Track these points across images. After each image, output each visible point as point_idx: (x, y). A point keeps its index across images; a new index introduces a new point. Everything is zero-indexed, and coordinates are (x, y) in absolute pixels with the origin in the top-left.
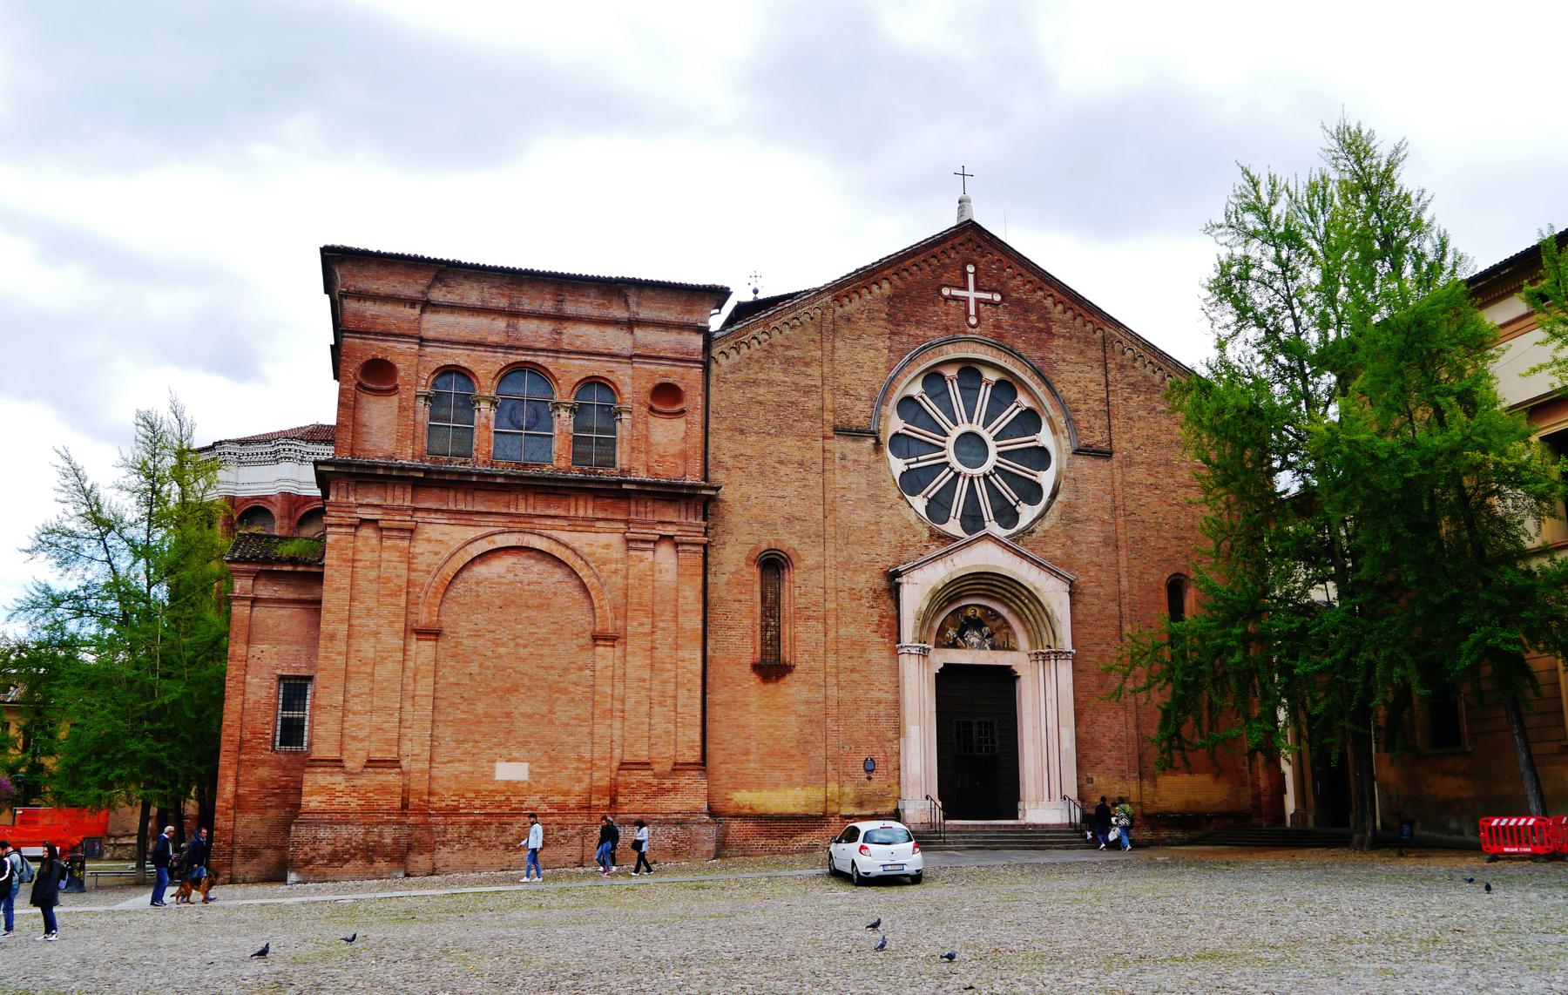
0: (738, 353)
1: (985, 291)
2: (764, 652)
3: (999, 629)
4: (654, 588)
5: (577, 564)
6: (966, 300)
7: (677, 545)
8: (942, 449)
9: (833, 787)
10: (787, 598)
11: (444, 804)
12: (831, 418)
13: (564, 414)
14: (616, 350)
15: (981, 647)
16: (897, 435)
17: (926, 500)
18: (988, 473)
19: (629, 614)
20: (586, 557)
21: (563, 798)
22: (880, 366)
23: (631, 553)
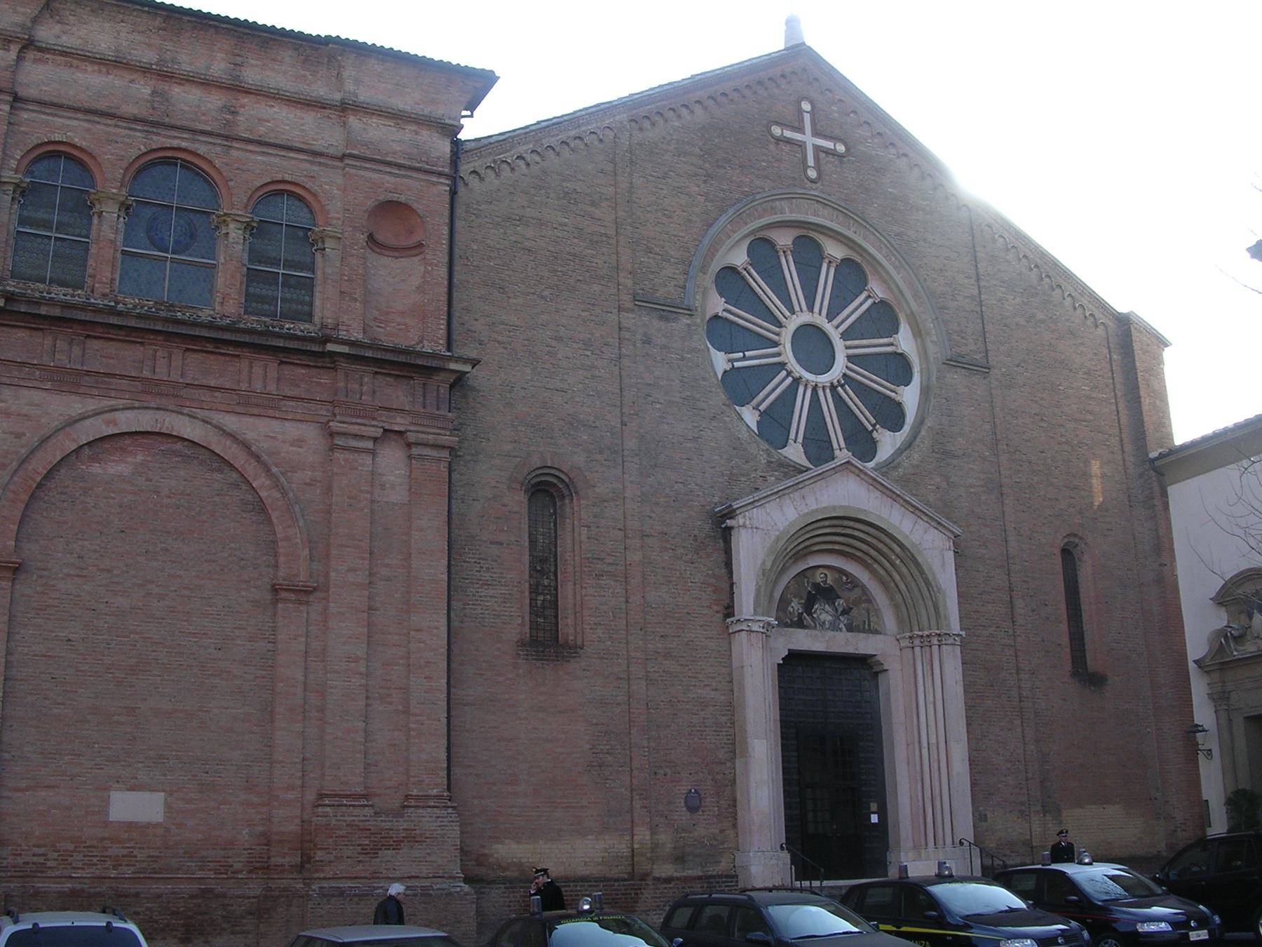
0: (498, 175)
1: (826, 137)
2: (534, 626)
3: (857, 602)
4: (372, 511)
5: (250, 469)
6: (801, 145)
7: (409, 445)
8: (776, 344)
9: (643, 835)
10: (569, 541)
11: (20, 861)
12: (629, 283)
13: (235, 232)
14: (319, 145)
15: (834, 627)
16: (716, 317)
17: (757, 413)
18: (836, 383)
19: (334, 552)
20: (265, 457)
21: (223, 853)
22: (694, 218)
23: (337, 454)
